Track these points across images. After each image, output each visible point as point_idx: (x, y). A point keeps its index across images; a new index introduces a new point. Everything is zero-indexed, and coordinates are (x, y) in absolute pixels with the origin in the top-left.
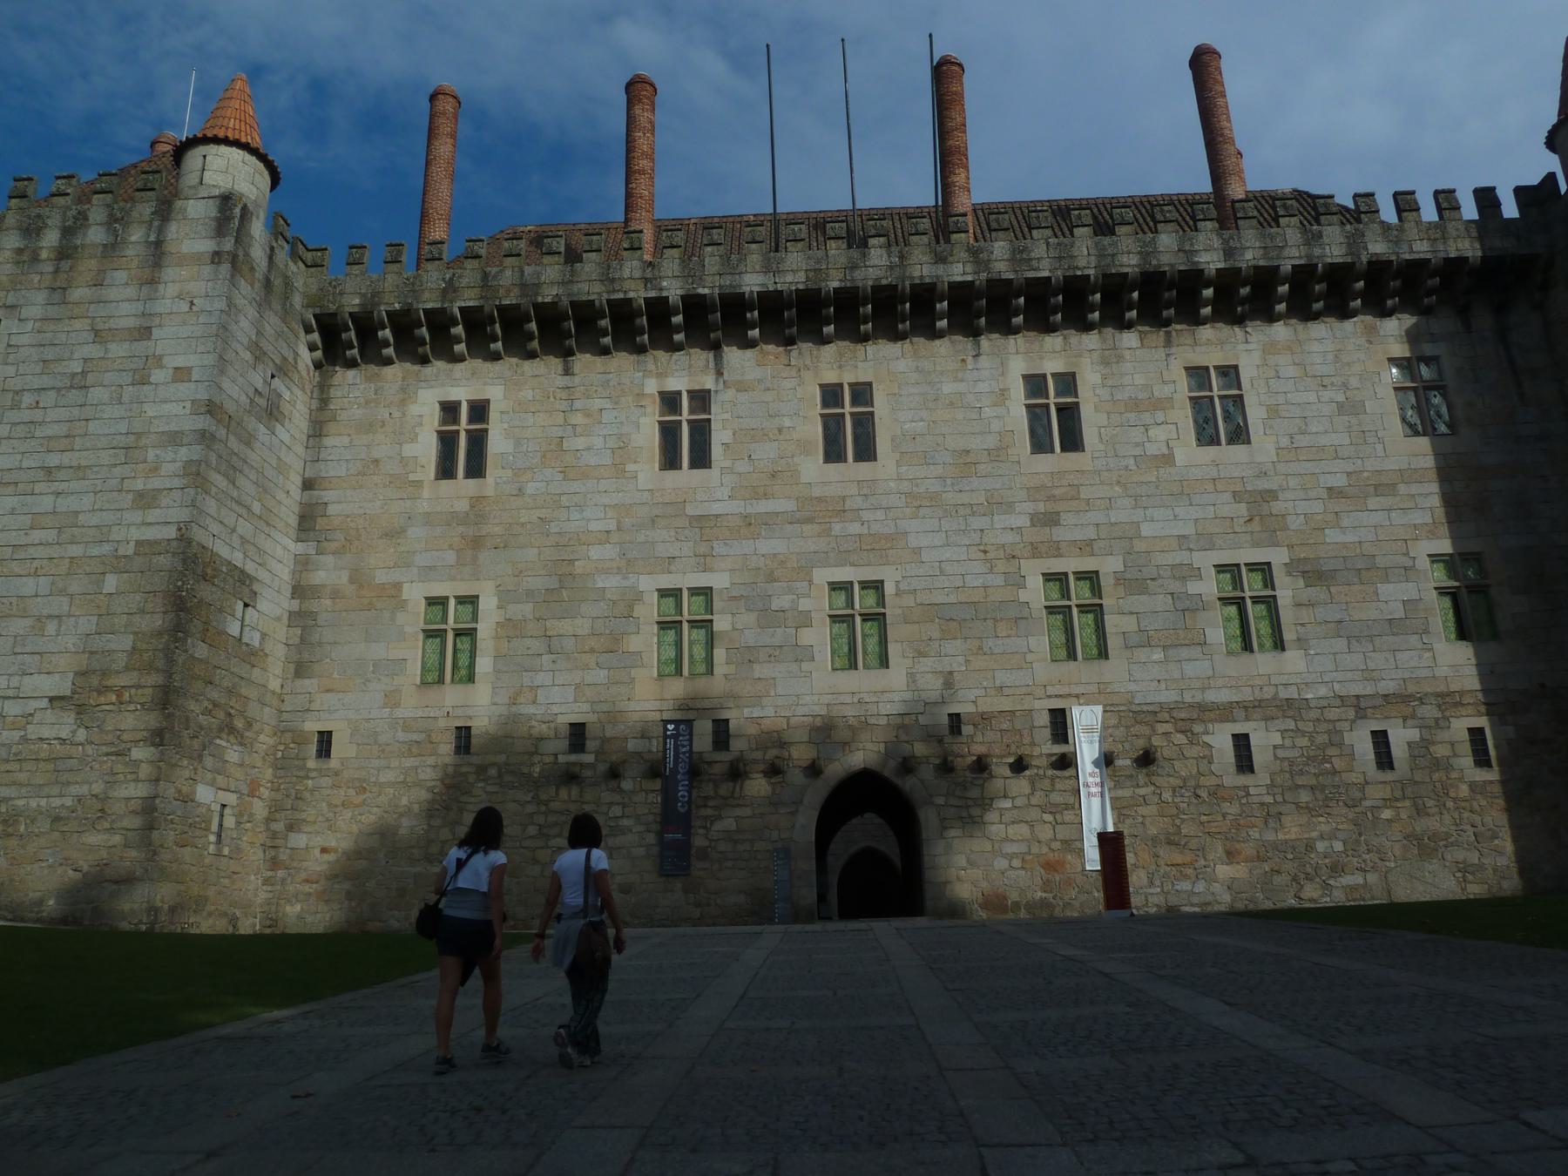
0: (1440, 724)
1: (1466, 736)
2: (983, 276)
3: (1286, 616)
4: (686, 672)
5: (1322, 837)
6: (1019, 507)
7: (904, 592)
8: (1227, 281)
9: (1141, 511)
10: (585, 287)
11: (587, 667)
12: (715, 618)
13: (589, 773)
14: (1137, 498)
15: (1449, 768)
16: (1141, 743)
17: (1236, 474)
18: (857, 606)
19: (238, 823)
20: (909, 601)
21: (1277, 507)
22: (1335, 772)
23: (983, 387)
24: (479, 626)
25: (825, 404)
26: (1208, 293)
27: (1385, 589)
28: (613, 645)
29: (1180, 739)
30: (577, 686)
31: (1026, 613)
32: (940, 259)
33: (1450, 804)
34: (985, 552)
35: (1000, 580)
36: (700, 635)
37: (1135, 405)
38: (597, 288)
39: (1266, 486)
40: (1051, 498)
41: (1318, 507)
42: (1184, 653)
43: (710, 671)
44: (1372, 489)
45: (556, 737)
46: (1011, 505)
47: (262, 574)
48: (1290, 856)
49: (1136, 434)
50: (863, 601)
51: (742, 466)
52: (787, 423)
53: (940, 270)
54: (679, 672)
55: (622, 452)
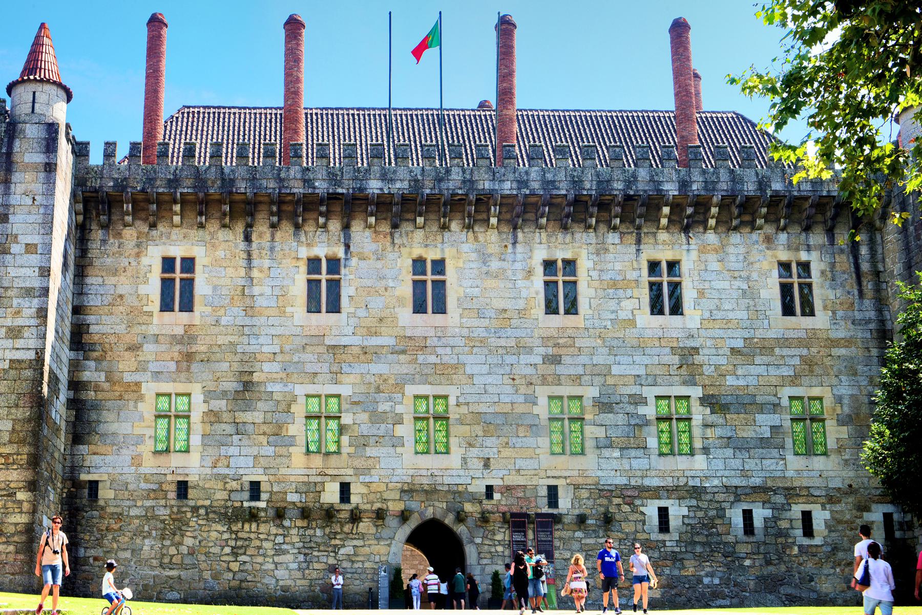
0: (786, 507)
1: (800, 516)
3: (697, 432)
4: (323, 451)
5: (707, 576)
6: (536, 350)
7: (462, 404)
9: (612, 357)
11: (261, 445)
12: (342, 415)
13: (263, 514)
14: (611, 348)
15: (787, 536)
16: (602, 509)
17: (674, 336)
18: (431, 412)
20: (464, 410)
21: (698, 359)
22: (719, 535)
24: (193, 414)
27: (759, 417)
29: (626, 508)
30: (255, 457)
31: (537, 423)
33: (786, 559)
34: (513, 379)
35: (521, 399)
36: (333, 424)
37: (614, 284)
39: (693, 344)
40: (557, 345)
41: (723, 361)
42: (633, 453)
43: (338, 453)
44: (758, 351)
45: (242, 490)
46: (531, 348)
48: (687, 586)
49: (612, 305)
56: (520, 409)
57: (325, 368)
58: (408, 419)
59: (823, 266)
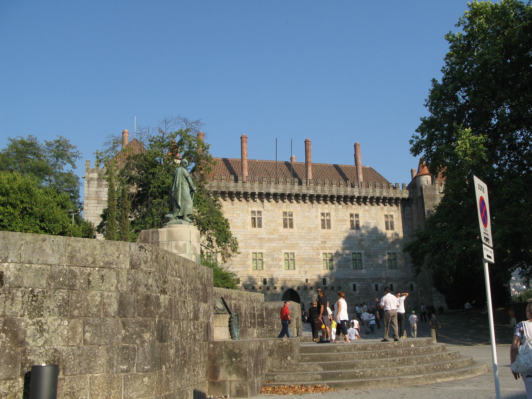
2: (316, 193)
3: (363, 263)
6: (320, 240)
8: (359, 198)
10: (239, 188)
11: (239, 267)
20: (299, 257)
23: (313, 215)
25: (284, 216)
26: (355, 200)
28: (244, 263)
29: (345, 285)
32: (308, 189)
35: (315, 254)
36: (260, 262)
37: (340, 220)
38: (241, 189)
40: (325, 238)
43: (263, 269)
49: (340, 226)
50: (291, 256)
51: (268, 228)
52: (277, 219)
53: (308, 191)
54: (257, 269)
55: (244, 222)
56: (315, 257)
57: (258, 244)
58: (283, 260)
59: (396, 216)
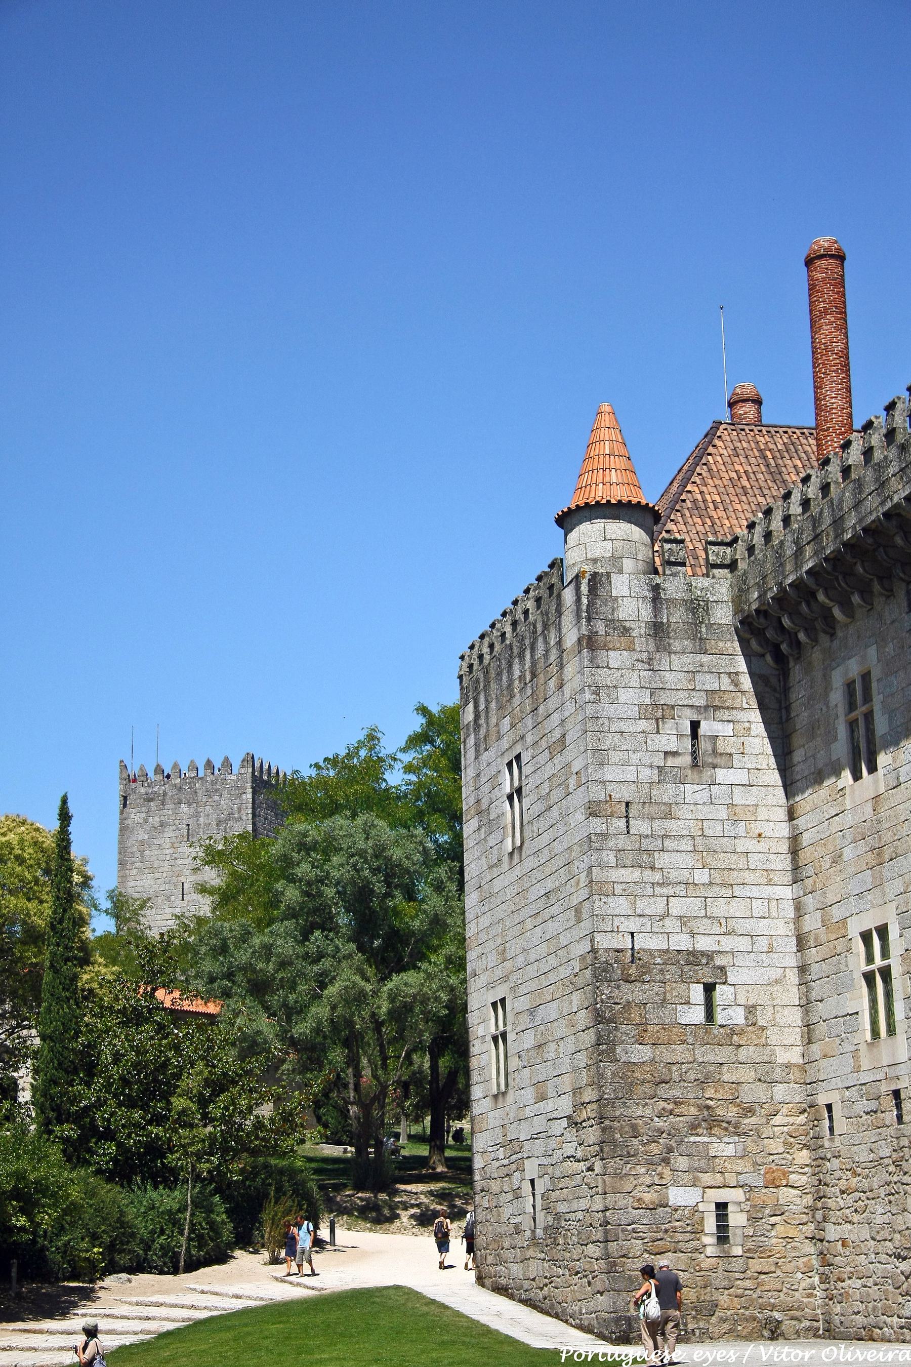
19: (754, 1219)
47: (728, 943)
